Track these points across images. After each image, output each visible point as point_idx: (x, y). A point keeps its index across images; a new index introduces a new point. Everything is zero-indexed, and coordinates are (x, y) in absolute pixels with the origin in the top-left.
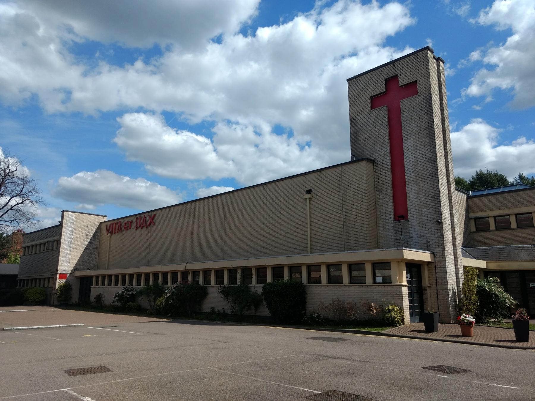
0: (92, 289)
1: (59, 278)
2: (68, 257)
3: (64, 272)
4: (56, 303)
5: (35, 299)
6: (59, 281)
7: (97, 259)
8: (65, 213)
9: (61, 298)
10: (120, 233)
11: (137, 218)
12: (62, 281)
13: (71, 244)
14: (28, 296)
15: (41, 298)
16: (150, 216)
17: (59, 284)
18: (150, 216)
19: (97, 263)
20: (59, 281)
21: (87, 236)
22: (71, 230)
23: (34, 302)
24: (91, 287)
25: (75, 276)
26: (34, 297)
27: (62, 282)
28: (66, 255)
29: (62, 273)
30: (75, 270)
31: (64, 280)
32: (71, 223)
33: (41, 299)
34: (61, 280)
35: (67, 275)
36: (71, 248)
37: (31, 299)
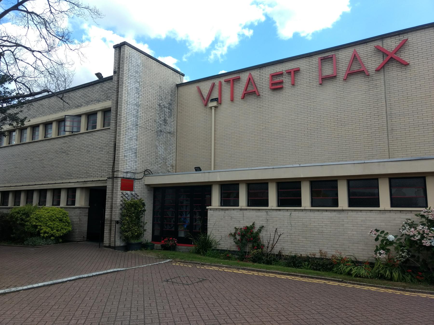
0: (210, 213)
1: (122, 189)
2: (133, 144)
3: (129, 176)
4: (119, 243)
5: (55, 231)
6: (122, 194)
7: (175, 154)
8: (127, 48)
9: (130, 232)
10: (252, 101)
11: (323, 60)
12: (127, 194)
13: (137, 117)
14: (37, 226)
15: (66, 229)
16: (379, 50)
17: (121, 201)
18: (379, 50)
19: (175, 162)
20: (122, 194)
21: (159, 105)
22: (137, 88)
23: (52, 238)
24: (207, 207)
25: (146, 185)
26: (51, 228)
27: (127, 196)
28: (131, 139)
29: (125, 175)
30: (146, 173)
31: (129, 192)
32: (137, 72)
33: (65, 232)
34: (125, 192)
35: (133, 181)
36: (137, 125)
37: (45, 232)
